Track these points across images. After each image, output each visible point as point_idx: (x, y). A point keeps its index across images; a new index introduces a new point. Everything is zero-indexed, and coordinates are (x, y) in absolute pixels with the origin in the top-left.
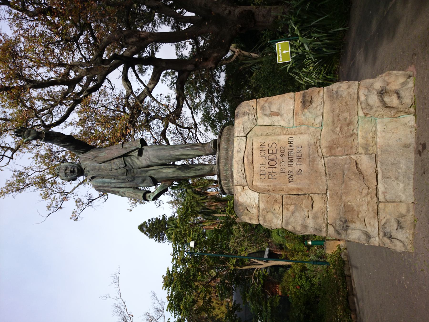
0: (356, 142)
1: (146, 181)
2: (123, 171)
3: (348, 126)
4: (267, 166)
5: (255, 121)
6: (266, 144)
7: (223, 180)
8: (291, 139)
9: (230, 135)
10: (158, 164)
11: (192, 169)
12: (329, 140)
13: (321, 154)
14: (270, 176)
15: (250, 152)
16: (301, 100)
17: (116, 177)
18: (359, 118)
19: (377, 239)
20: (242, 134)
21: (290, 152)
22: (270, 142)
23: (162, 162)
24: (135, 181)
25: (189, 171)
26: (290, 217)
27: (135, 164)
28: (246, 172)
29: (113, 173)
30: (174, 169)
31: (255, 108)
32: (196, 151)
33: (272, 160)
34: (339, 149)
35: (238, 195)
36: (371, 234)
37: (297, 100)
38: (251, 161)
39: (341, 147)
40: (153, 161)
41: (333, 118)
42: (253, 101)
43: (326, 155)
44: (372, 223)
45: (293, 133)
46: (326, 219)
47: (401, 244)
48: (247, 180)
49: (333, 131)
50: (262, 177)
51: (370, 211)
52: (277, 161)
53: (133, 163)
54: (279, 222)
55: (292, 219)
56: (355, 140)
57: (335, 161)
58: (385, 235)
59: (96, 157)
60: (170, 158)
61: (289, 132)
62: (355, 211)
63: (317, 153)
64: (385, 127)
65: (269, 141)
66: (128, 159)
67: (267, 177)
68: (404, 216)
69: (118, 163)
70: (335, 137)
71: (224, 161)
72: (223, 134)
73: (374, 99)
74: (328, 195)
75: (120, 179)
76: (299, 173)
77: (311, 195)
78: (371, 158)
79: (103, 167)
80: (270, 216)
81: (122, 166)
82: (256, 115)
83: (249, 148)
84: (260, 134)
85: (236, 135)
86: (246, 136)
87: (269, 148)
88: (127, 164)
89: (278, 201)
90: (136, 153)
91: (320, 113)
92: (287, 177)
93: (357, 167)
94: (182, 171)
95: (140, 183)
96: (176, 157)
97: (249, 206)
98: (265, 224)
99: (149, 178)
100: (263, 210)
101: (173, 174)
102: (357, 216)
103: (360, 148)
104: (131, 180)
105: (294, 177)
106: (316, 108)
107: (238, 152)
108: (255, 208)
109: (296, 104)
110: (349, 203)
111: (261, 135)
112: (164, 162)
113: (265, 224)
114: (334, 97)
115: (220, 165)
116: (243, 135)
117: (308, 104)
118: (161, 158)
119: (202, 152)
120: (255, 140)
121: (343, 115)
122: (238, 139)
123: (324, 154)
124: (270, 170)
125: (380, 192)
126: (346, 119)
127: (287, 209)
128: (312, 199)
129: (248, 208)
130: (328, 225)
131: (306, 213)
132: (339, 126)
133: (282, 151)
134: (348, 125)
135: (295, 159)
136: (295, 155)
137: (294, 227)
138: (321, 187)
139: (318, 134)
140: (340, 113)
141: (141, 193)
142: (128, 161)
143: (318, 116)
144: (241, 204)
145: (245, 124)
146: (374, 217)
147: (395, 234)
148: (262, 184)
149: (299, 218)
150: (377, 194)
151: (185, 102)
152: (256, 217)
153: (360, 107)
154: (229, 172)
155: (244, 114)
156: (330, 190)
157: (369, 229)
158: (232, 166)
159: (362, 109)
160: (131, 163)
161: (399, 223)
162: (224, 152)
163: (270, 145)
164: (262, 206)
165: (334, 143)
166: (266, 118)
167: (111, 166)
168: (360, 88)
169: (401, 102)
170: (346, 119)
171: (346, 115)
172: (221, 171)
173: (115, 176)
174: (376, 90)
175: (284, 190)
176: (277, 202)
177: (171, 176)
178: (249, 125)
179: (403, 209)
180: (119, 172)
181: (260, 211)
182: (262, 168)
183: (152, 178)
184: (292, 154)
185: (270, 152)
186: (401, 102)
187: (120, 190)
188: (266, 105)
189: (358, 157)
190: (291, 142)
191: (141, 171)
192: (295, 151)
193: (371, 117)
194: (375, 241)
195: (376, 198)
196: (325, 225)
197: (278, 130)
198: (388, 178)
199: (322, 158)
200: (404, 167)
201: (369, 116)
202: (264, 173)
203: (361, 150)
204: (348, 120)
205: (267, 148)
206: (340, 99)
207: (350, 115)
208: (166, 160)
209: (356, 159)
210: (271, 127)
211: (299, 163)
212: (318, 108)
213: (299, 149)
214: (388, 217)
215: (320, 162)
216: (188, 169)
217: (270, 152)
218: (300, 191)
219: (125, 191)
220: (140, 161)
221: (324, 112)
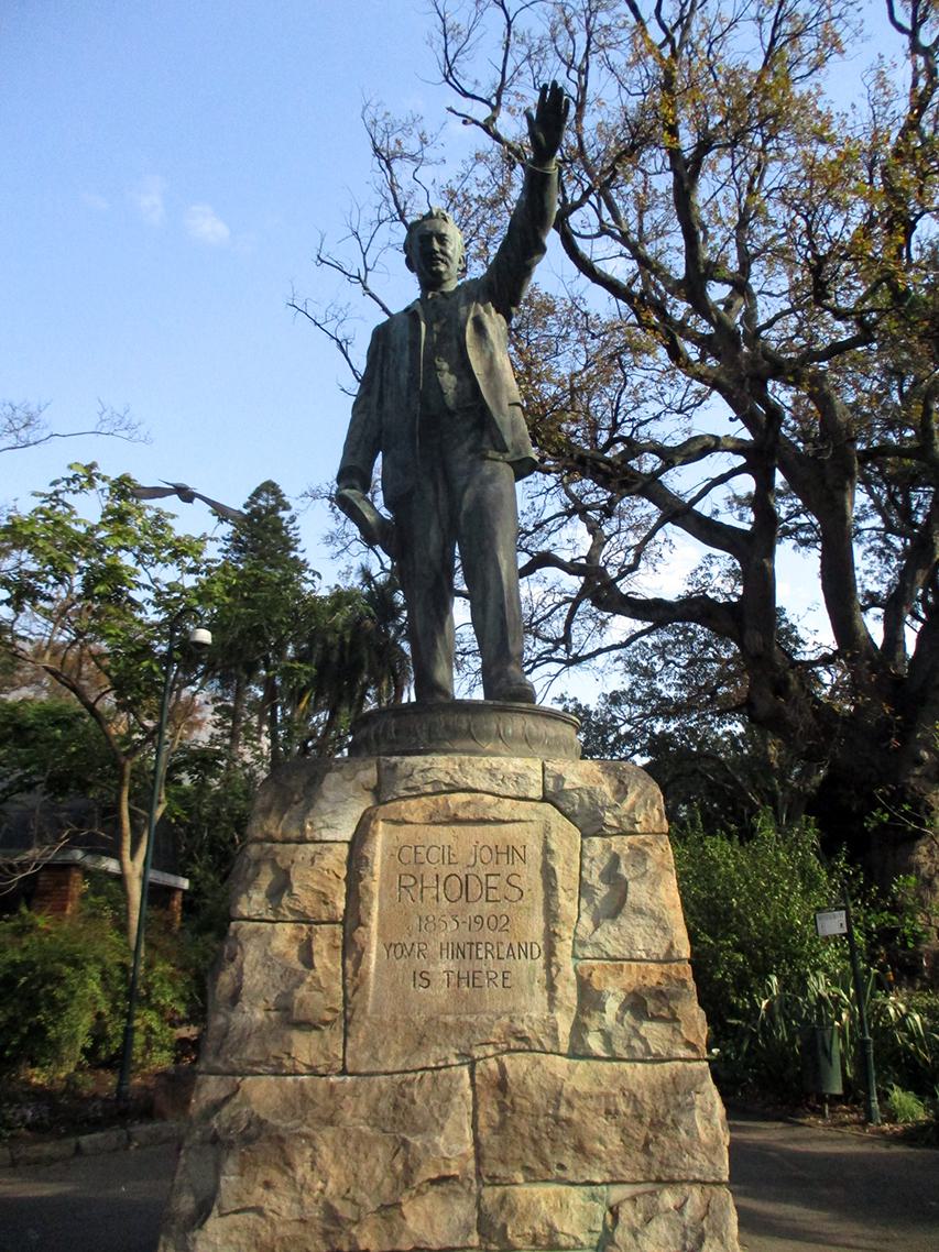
4: (445, 871)
6: (519, 866)
8: (536, 950)
13: (482, 1055)
15: (492, 814)
21: (489, 947)
22: (524, 879)
23: (462, 523)
33: (465, 887)
35: (345, 772)
38: (461, 814)
50: (408, 853)
57: (456, 1100)
67: (403, 869)
74: (342, 1078)
75: (409, 395)
76: (419, 980)
83: (507, 808)
86: (544, 799)
105: (403, 961)
110: (308, 1152)
123: (480, 1063)
124: (430, 881)
130: (239, 1079)
133: (493, 919)
151: (649, 624)
153: (640, 1189)
156: (355, 1087)
159: (633, 1199)
163: (514, 880)
165: (518, 1100)
185: (492, 881)
187: (374, 399)
202: (422, 857)
211: (454, 980)
215: (453, 1050)
217: (492, 881)
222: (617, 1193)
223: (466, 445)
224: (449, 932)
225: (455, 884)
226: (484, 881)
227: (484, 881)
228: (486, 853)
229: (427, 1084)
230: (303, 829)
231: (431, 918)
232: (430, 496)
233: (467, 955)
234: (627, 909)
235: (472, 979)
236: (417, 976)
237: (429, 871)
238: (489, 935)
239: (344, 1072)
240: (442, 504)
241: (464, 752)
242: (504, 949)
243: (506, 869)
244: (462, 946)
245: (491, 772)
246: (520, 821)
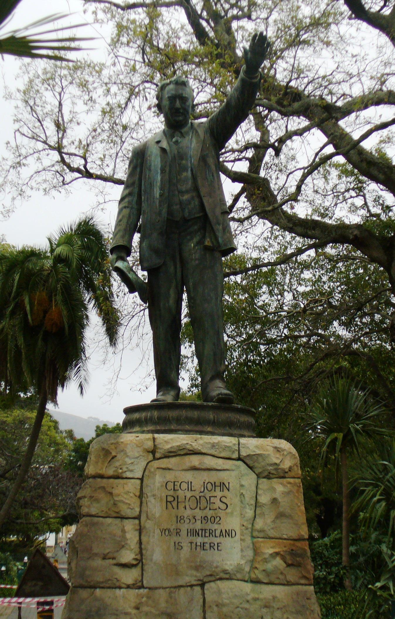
5: (266, 474)
20: (244, 453)
27: (189, 237)
31: (286, 475)
50: (170, 486)
65: (232, 498)
75: (160, 206)
77: (141, 564)
79: (185, 174)
81: (186, 214)
82: (274, 476)
84: (243, 483)
86: (239, 459)
87: (219, 498)
91: (273, 578)
92: (169, 527)
106: (282, 573)
109: (290, 542)
111: (242, 486)
120: (233, 474)
122: (234, 444)
133: (213, 519)
139: (239, 576)
140: (272, 610)
162: (211, 417)
163: (224, 499)
177: (162, 306)
182: (184, 486)
190: (228, 533)
199: (200, 583)
205: (218, 493)
210: (253, 502)
212: (281, 576)
213: (216, 547)
223: (195, 240)
226: (208, 499)
227: (208, 499)
228: (209, 486)
231: (182, 517)
232: (172, 269)
236: (176, 544)
240: (179, 274)
244: (197, 531)
245: (213, 446)
246: (228, 470)
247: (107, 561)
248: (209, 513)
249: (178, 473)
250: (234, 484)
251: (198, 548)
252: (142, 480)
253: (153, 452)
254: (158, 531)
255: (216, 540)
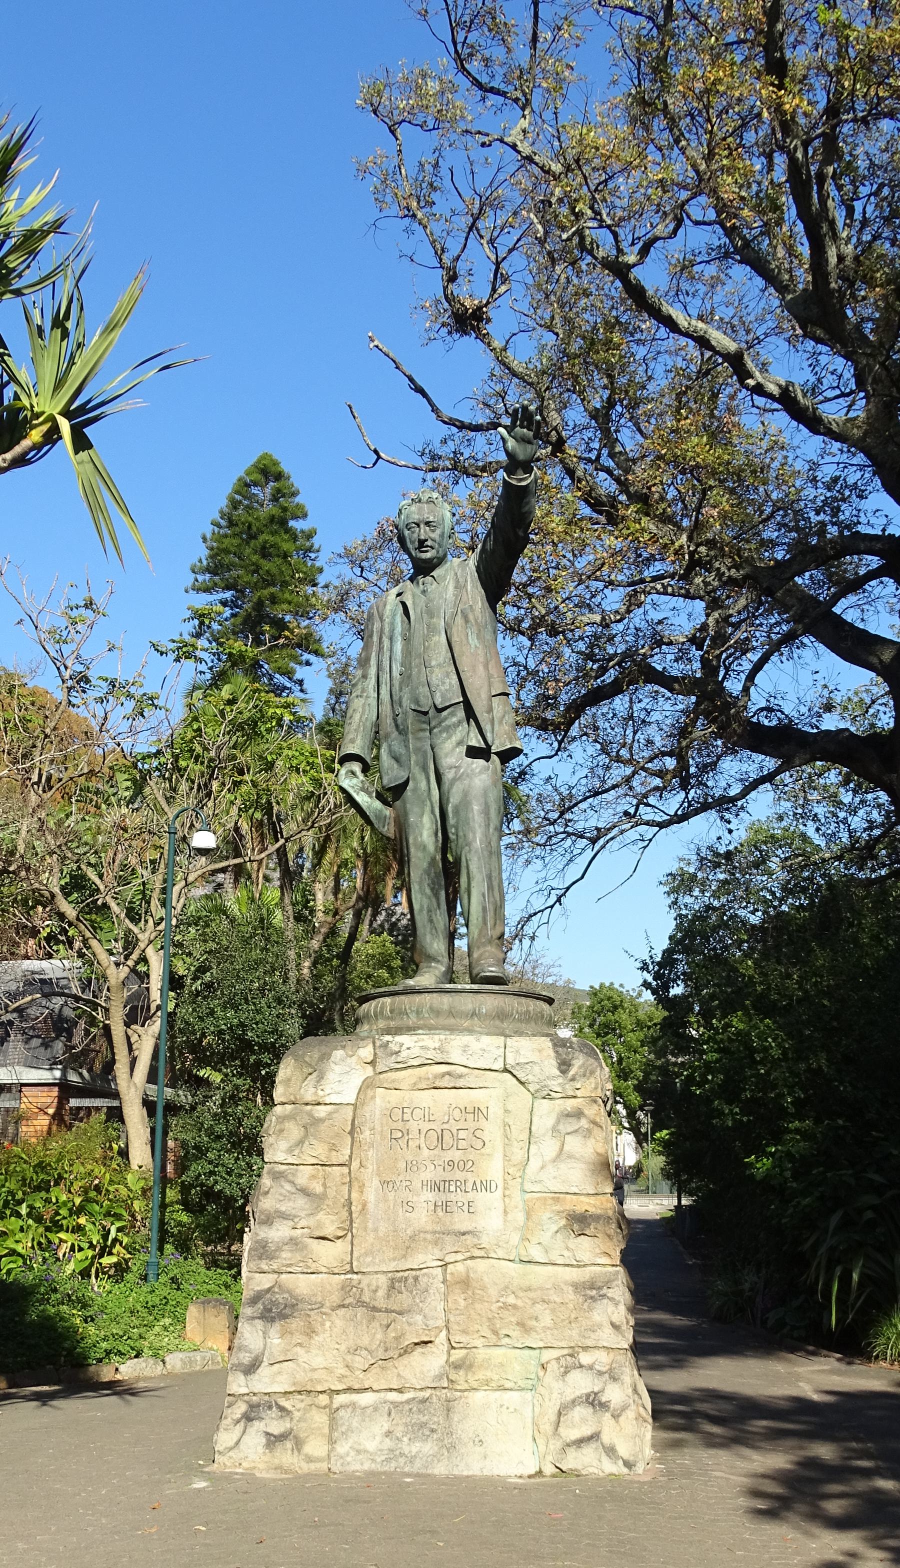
0: (479, 1343)
1: (396, 766)
2: (422, 700)
3: (518, 1324)
6: (483, 1123)
7: (392, 1004)
9: (520, 1021)
10: (444, 802)
11: (434, 900)
12: (485, 1279)
14: (400, 1135)
16: (592, 1210)
17: (406, 677)
18: (538, 1351)
19: (246, 1391)
20: (510, 1061)
23: (450, 815)
24: (395, 734)
25: (428, 891)
26: (292, 1183)
27: (444, 735)
28: (409, 1070)
29: (419, 672)
30: (431, 848)
31: (578, 1093)
32: (480, 919)
34: (462, 1303)
35: (348, 1048)
36: (255, 1377)
37: (592, 1200)
38: (437, 1084)
39: (466, 1307)
40: (454, 790)
41: (541, 1289)
42: (596, 1088)
43: (449, 1271)
44: (279, 1378)
45: (507, 1193)
46: (289, 1270)
47: (231, 1444)
48: (389, 1074)
49: (507, 1287)
51: (309, 1374)
52: (436, 1152)
53: (447, 729)
54: (280, 1157)
55: (288, 1186)
56: (482, 1340)
57: (431, 1291)
58: (252, 1407)
59: (466, 620)
60: (460, 841)
61: (510, 1183)
62: (311, 1337)
63: (455, 1249)
64: (511, 1409)
65: (492, 1131)
66: (461, 713)
67: (395, 1125)
68: (299, 1451)
69: (445, 688)
70: (493, 1292)
71: (446, 1007)
72: (523, 1000)
73: (581, 1383)
74: (349, 1276)
75: (401, 689)
78: (439, 1377)
80: (294, 1131)
81: (438, 701)
82: (560, 1095)
85: (509, 1041)
86: (506, 1070)
88: (445, 713)
89: (334, 1153)
90: (475, 741)
92: (394, 1178)
93: (416, 1344)
94: (427, 872)
95: (390, 746)
96: (463, 859)
97: (321, 1078)
98: (274, 1118)
99: (402, 775)
100: (310, 1114)
101: (415, 844)
102: (300, 1344)
103: (464, 1351)
104: (399, 722)
105: (393, 1193)
106: (568, 1248)
107: (465, 1049)
108: (316, 1093)
109: (583, 1198)
110: (328, 1324)
111: (506, 1111)
112: (451, 821)
113: (274, 1118)
114: (591, 1290)
115: (435, 995)
116: (508, 1061)
117: (576, 1227)
118: (462, 814)
119: (476, 936)
121: (547, 1311)
124: (414, 1134)
125: (354, 1397)
126: (536, 1319)
127: (313, 1177)
128: (339, 1238)
129: (315, 1075)
131: (303, 1223)
132: (519, 1303)
134: (521, 1324)
135: (443, 1197)
136: (452, 1197)
137: (267, 1193)
138: (369, 1259)
140: (551, 1306)
141: (363, 748)
142: (452, 714)
143: (547, 1252)
144: (325, 1057)
145: (536, 1069)
146: (294, 1384)
147: (258, 1426)
148: (377, 1112)
149: (291, 1204)
150: (349, 1390)
152: (292, 1098)
154: (412, 1020)
155: (564, 1066)
157: (264, 1371)
158: (431, 1028)
159: (558, 1359)
160: (448, 722)
161: (282, 1437)
162: (470, 1006)
163: (478, 1133)
164: (321, 1112)
166: (550, 1122)
167: (439, 665)
168: (612, 1354)
169: (568, 1445)
170: (536, 1319)
171: (546, 1319)
172: (417, 998)
173: (409, 677)
174: (602, 1391)
175: (362, 1170)
176: (331, 1150)
177: (411, 841)
178: (531, 1076)
179: (316, 1447)
180: (421, 689)
181: (309, 1107)
183: (406, 783)
184: (452, 1188)
185: (462, 1135)
186: (568, 1445)
188: (584, 1122)
189: (441, 1347)
190: (486, 1186)
191: (425, 752)
192: (460, 1197)
193: (539, 1379)
194: (238, 1384)
195: (340, 1387)
196: (275, 1267)
197: (518, 1155)
198: (389, 1414)
200: (414, 1450)
201: (541, 1373)
202: (406, 1117)
203: (457, 1355)
204: (534, 1323)
206: (585, 1307)
207: (546, 1329)
208: (457, 829)
209: (437, 1341)
212: (566, 1253)
213: (465, 1208)
214: (297, 1415)
216: (432, 889)
217: (462, 1135)
218: (360, 1207)
219: (367, 697)
220: (453, 749)
221: (556, 1268)
222: (547, 1355)
223: (455, 739)
224: (429, 1174)
225: (433, 1135)
229: (411, 1280)
230: (316, 1093)
233: (442, 1189)
234: (563, 1157)
235: (446, 1207)
237: (413, 1126)
238: (459, 1175)
239: (352, 1272)
241: (445, 1028)
242: (470, 1185)
243: (472, 1125)
247: (299, 1232)
248: (457, 1155)
249: (407, 1095)
250: (495, 1111)
251: (439, 1210)
252: (355, 1106)
253: (373, 1063)
254: (376, 1182)
255: (460, 1197)
